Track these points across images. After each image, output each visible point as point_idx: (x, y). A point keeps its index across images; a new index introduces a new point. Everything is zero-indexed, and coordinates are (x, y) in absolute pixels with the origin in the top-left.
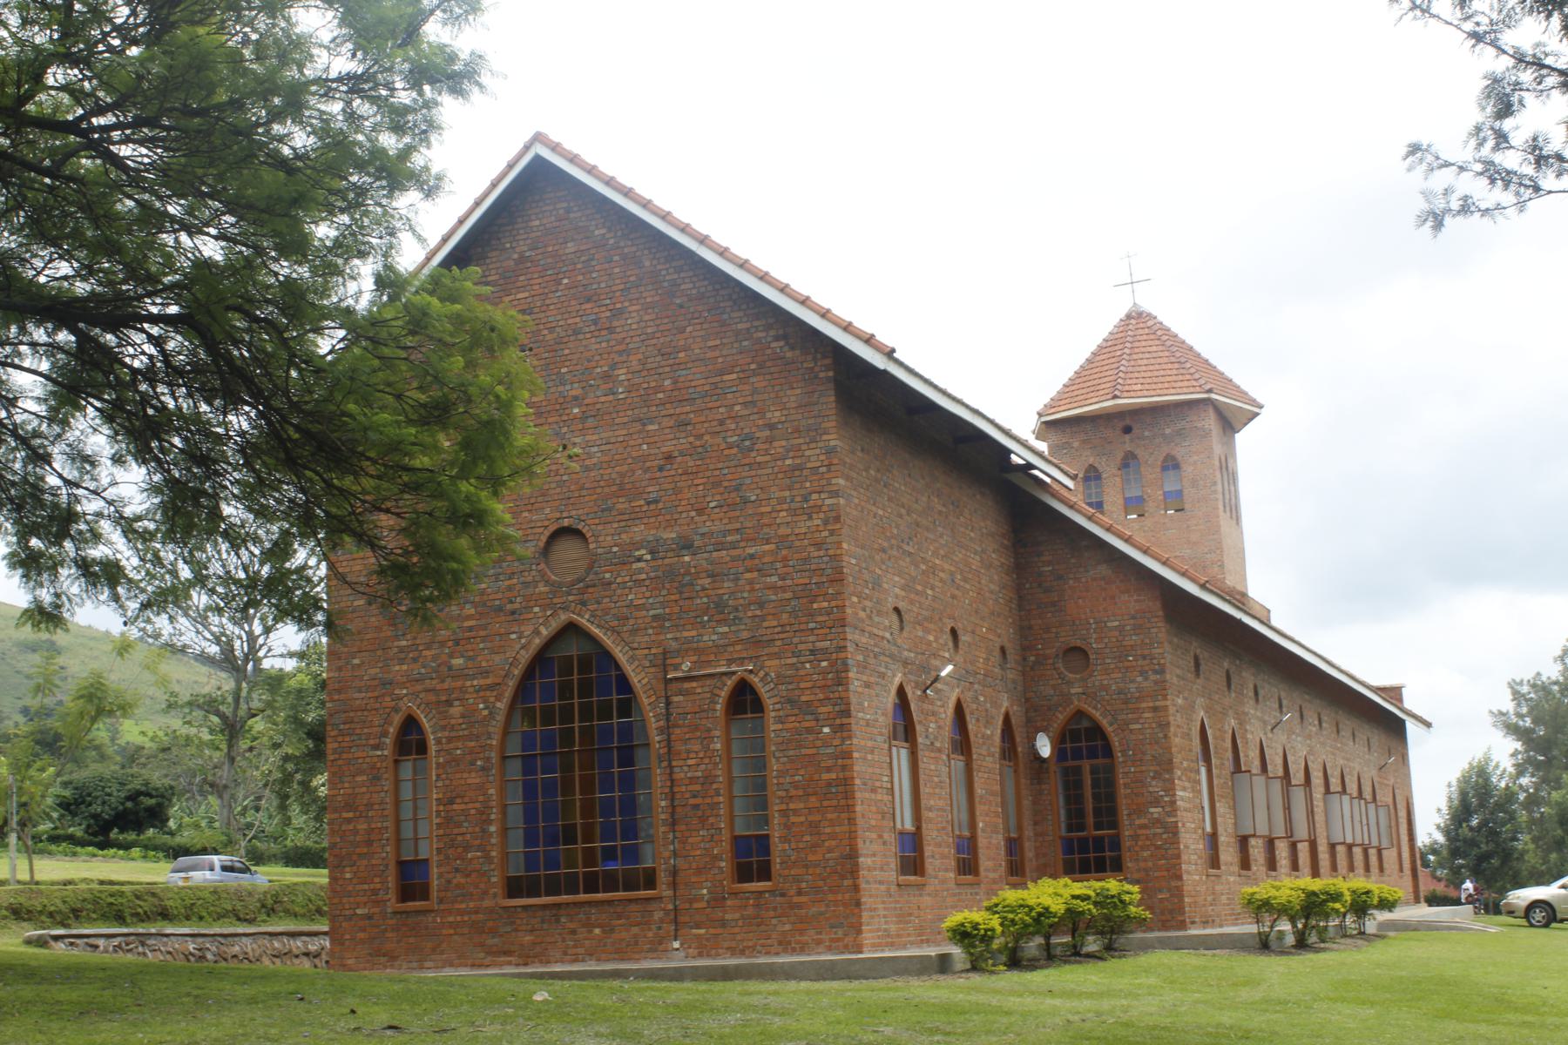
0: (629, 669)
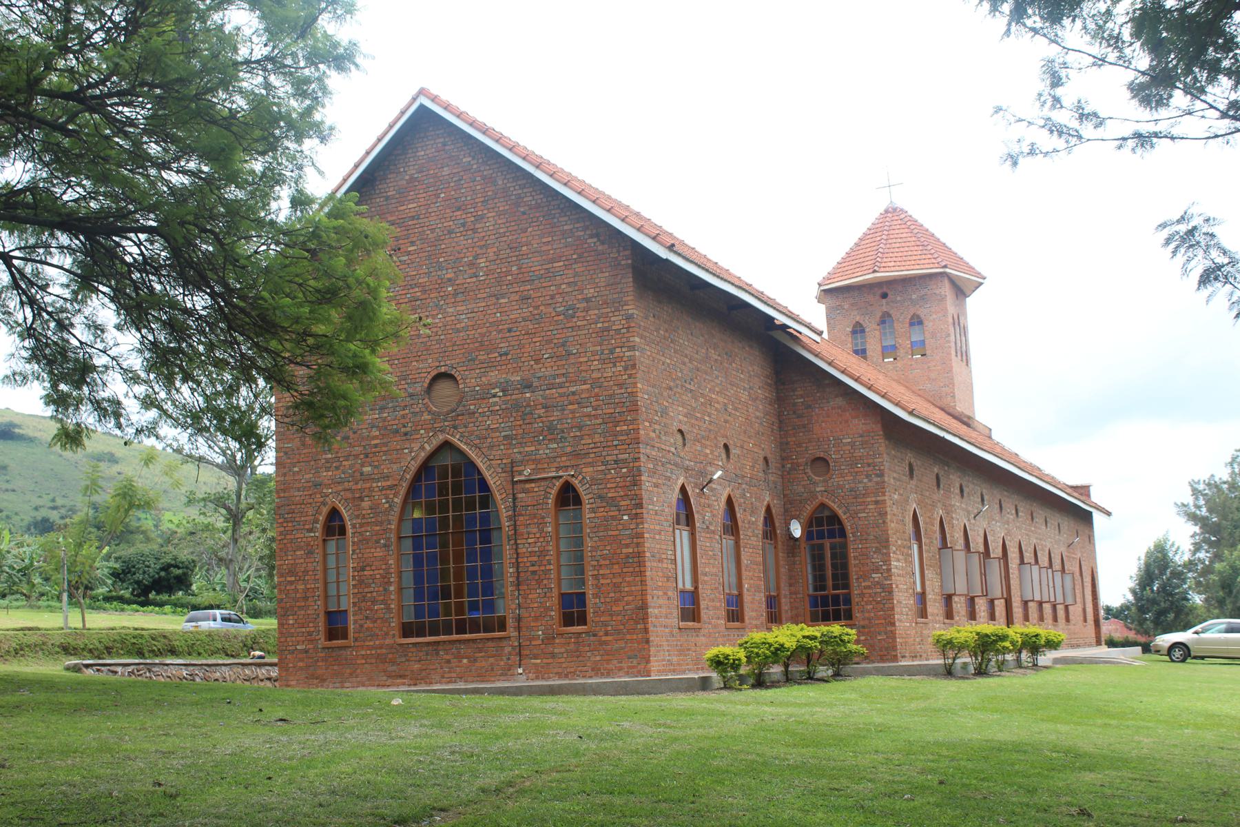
0: (487, 474)
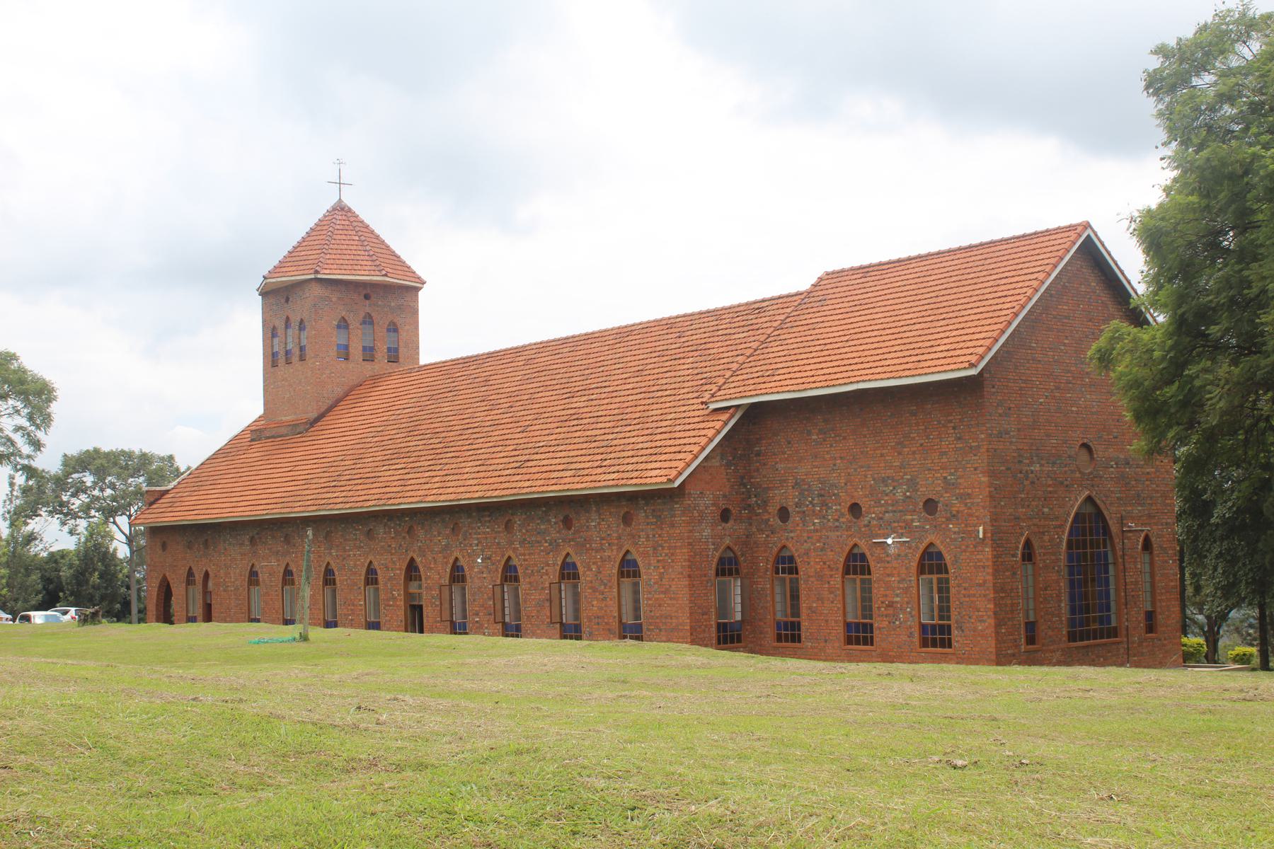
0: (1110, 523)
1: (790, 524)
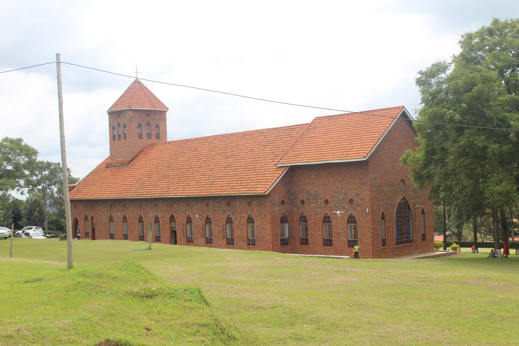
1: (305, 206)
